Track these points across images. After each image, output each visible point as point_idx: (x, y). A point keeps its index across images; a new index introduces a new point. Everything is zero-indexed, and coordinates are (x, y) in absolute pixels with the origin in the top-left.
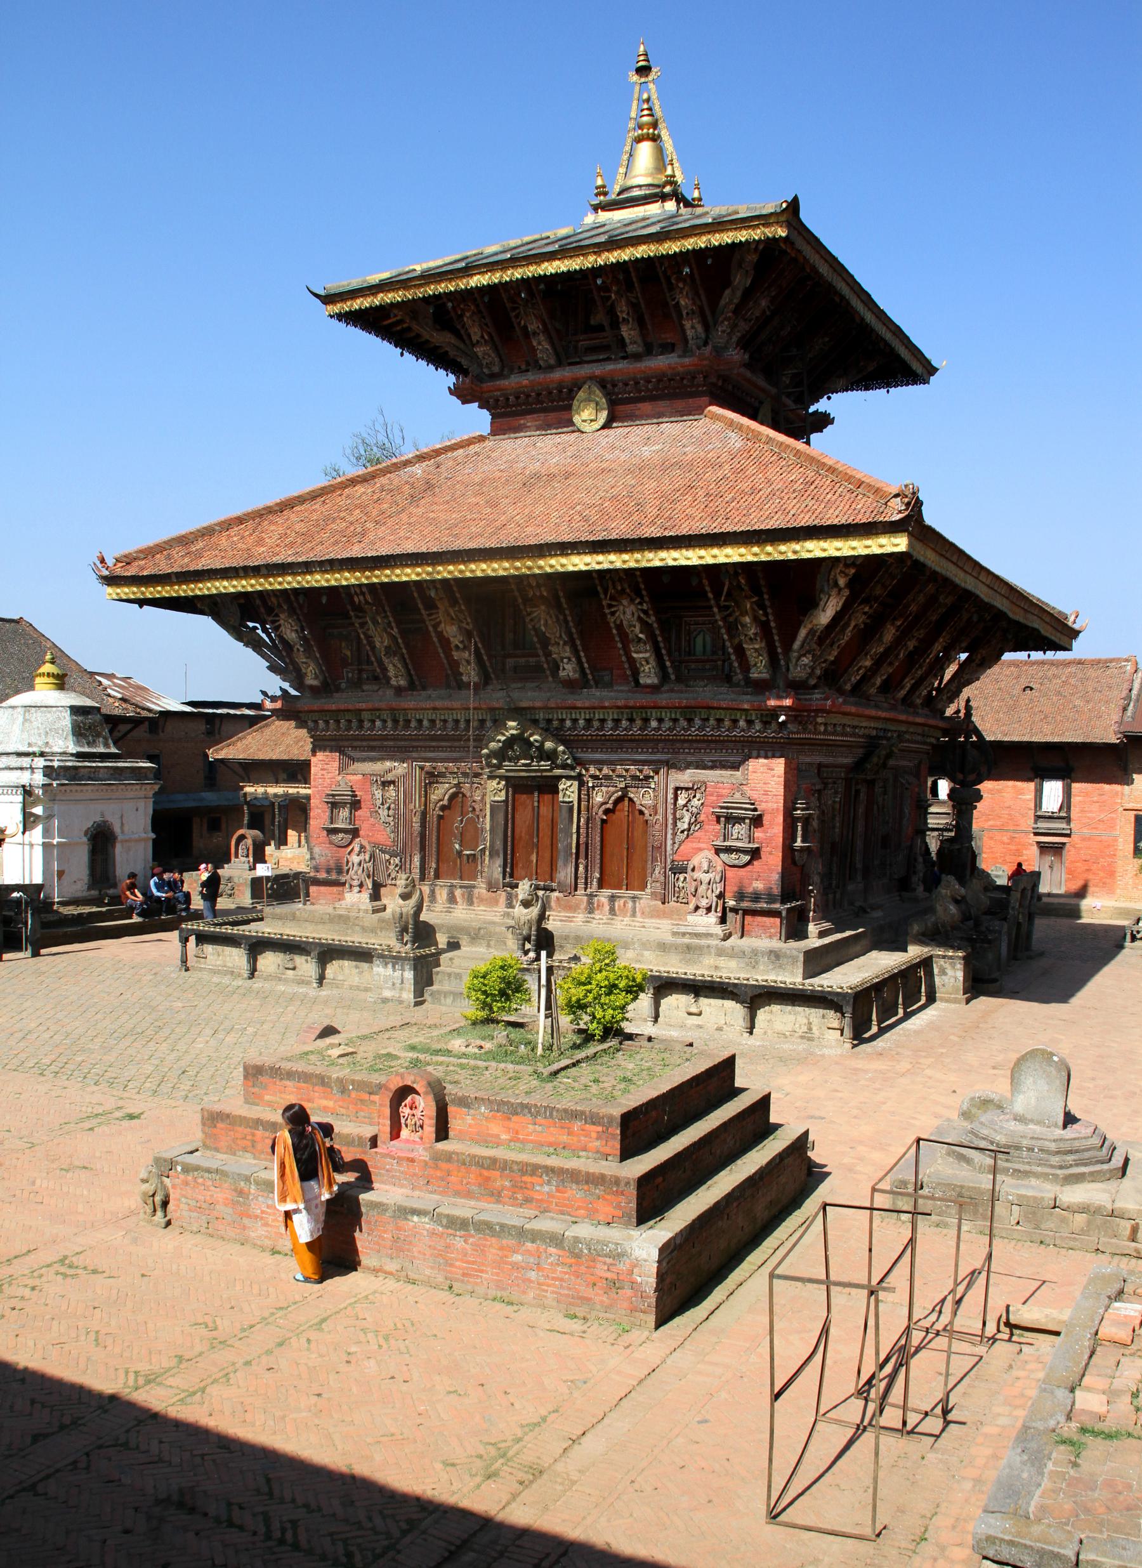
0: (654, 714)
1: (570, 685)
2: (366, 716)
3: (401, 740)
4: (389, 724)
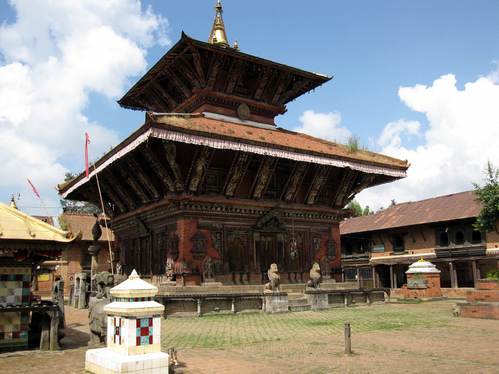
0: (312, 213)
1: (289, 202)
2: (215, 205)
3: (224, 216)
4: (224, 210)
